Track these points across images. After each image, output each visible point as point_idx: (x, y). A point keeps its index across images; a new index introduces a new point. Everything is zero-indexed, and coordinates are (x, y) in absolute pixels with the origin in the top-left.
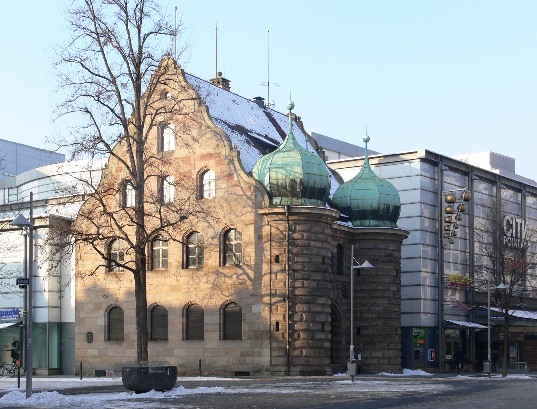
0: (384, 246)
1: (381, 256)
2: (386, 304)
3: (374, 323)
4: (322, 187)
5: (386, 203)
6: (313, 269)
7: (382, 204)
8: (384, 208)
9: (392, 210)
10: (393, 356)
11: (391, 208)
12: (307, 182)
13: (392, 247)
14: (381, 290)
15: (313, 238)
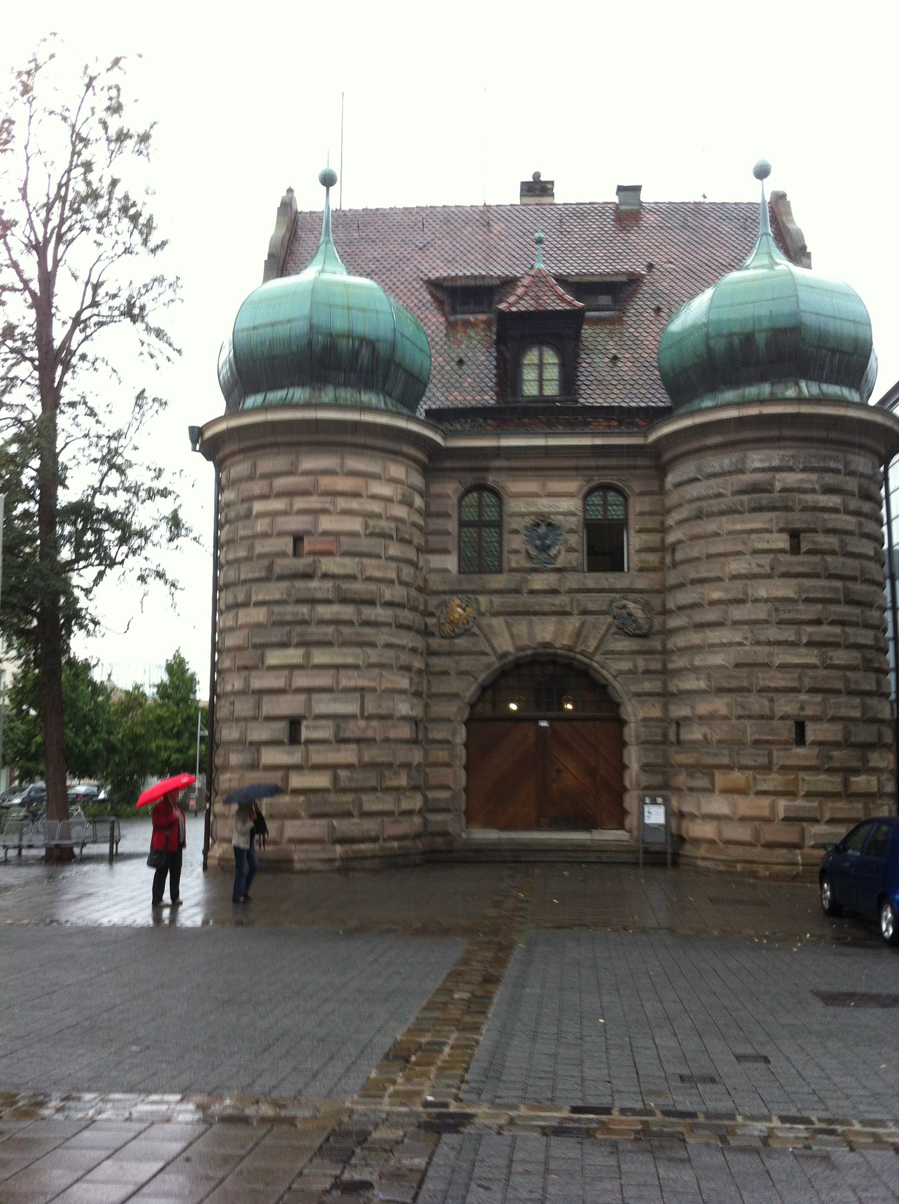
0: (726, 461)
1: (720, 495)
2: (740, 644)
10: (782, 815)
13: (762, 461)
14: (719, 602)
15: (257, 492)
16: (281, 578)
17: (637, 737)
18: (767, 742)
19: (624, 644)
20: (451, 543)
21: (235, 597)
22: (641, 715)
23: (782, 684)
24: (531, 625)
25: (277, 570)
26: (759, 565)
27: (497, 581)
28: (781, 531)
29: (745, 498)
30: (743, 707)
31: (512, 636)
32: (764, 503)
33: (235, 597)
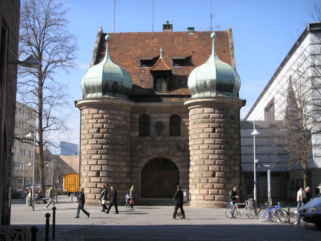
4: (99, 84)
5: (202, 79)
6: (90, 137)
7: (198, 80)
8: (201, 84)
9: (209, 83)
11: (208, 82)
12: (88, 84)
14: (198, 144)
16: (95, 138)
18: (207, 177)
19: (179, 154)
20: (137, 129)
21: (85, 142)
22: (183, 171)
23: (210, 163)
25: (94, 137)
26: (206, 136)
27: (148, 138)
28: (211, 127)
29: (204, 119)
30: (202, 169)
32: (207, 121)
33: (85, 142)
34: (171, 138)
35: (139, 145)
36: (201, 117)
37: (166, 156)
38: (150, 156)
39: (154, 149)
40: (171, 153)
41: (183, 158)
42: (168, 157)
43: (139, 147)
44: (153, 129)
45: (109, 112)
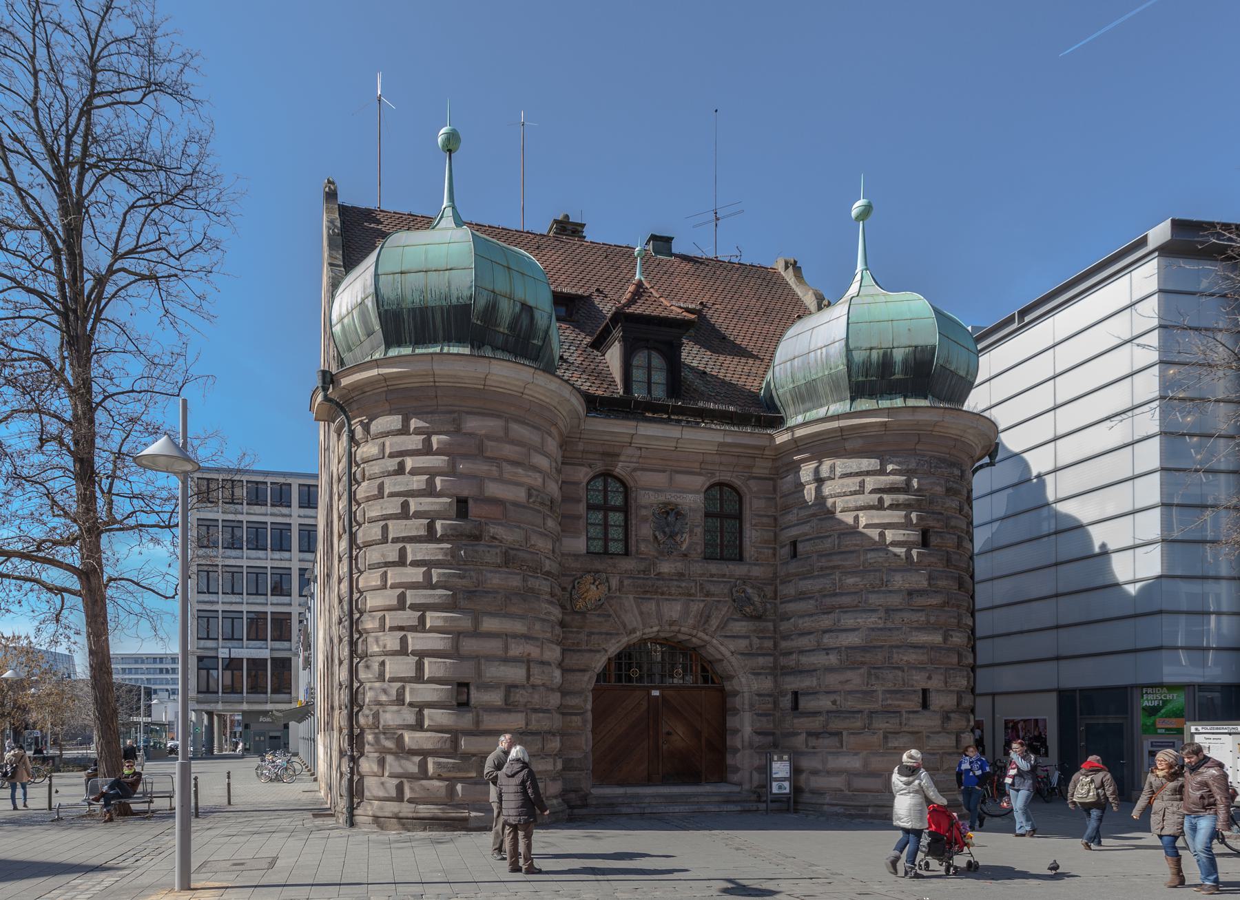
3: (832, 680)
17: (752, 706)
24: (658, 605)
31: (641, 613)
34: (714, 568)
35: (593, 587)
36: (869, 487)
37: (695, 632)
38: (634, 631)
39: (651, 607)
40: (714, 622)
41: (756, 641)
42: (701, 634)
43: (594, 592)
44: (644, 530)
45: (506, 430)
